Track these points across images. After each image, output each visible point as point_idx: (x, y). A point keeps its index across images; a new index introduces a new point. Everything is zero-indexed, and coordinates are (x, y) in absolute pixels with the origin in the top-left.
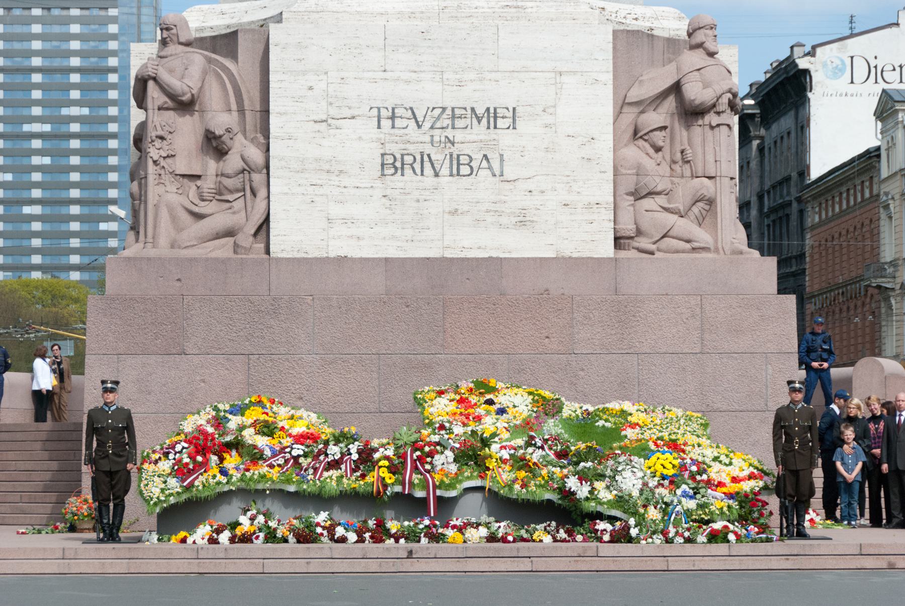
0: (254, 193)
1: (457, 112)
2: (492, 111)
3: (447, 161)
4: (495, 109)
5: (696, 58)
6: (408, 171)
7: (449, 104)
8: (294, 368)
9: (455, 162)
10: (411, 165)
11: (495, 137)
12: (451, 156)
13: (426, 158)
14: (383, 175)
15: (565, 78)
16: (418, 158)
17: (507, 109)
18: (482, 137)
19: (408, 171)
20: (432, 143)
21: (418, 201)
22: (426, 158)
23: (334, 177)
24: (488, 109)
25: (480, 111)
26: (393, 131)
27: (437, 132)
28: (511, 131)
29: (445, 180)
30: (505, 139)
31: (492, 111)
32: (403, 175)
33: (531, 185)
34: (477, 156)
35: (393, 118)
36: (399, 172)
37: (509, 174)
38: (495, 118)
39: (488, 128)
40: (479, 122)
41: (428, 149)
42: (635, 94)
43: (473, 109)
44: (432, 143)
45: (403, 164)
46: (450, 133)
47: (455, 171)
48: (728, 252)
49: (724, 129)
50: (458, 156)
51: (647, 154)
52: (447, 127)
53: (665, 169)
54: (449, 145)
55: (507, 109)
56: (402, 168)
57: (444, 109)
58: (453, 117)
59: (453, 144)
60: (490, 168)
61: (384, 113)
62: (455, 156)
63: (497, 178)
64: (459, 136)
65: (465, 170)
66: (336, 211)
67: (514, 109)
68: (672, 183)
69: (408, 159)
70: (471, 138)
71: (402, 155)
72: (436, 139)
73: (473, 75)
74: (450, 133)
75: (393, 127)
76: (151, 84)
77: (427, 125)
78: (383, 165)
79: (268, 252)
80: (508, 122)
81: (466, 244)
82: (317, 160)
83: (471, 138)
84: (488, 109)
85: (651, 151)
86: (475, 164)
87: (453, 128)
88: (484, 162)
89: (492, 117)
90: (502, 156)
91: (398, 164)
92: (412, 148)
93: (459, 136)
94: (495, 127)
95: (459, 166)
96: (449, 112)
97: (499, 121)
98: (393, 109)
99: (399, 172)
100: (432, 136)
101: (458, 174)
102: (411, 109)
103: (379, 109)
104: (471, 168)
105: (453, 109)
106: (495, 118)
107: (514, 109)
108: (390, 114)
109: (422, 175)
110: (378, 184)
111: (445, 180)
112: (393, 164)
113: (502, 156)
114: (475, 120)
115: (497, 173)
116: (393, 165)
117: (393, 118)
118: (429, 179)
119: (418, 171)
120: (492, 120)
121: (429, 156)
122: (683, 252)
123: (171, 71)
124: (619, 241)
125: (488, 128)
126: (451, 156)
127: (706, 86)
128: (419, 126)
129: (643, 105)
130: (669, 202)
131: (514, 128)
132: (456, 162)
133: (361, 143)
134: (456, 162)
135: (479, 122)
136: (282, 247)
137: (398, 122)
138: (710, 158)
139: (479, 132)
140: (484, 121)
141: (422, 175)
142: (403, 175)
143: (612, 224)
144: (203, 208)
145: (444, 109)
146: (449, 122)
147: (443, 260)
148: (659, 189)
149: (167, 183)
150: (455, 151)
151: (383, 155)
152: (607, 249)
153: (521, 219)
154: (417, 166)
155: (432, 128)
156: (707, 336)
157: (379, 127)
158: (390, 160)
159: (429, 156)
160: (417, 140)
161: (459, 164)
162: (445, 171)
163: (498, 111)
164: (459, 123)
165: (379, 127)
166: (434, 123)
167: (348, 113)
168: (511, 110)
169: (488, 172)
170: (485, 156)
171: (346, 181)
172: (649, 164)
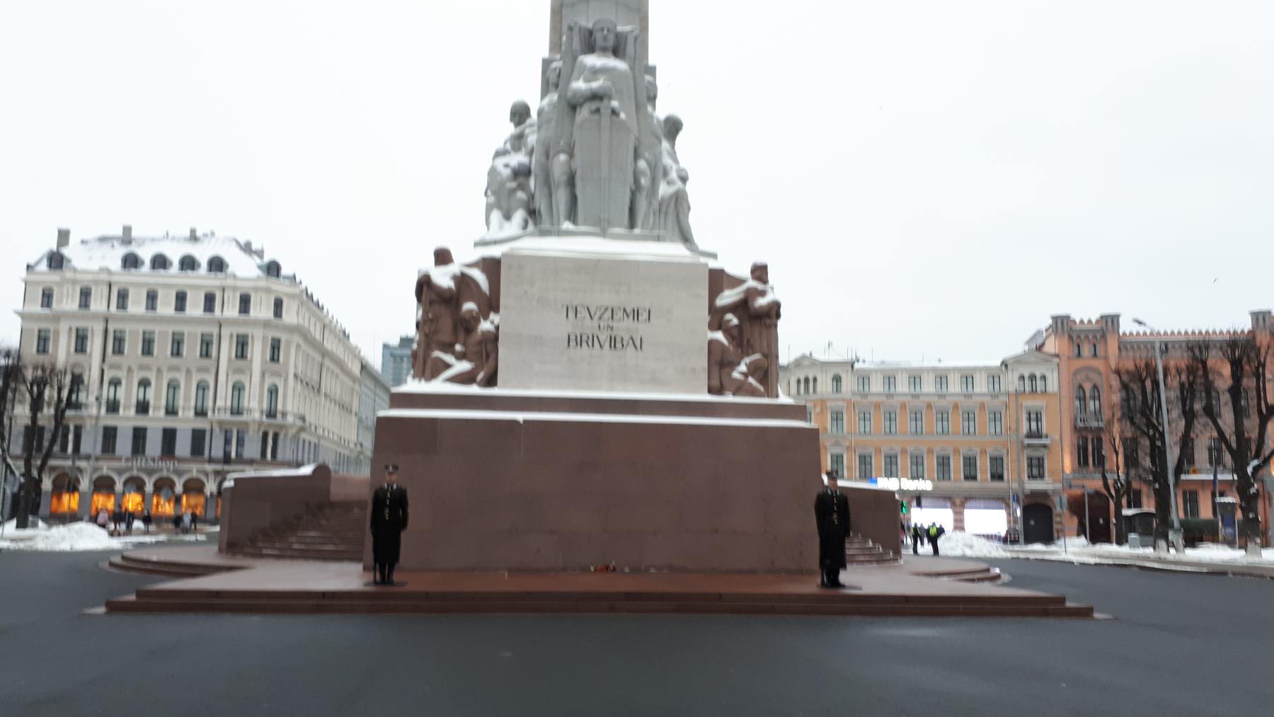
0: (488, 356)
19: (584, 344)
25: (629, 310)
41: (596, 332)
64: (615, 325)
69: (584, 338)
76: (425, 289)
77: (596, 318)
80: (646, 315)
83: (623, 326)
89: (636, 314)
116: (577, 340)
132: (613, 342)
138: (765, 344)
139: (629, 323)
160: (589, 326)
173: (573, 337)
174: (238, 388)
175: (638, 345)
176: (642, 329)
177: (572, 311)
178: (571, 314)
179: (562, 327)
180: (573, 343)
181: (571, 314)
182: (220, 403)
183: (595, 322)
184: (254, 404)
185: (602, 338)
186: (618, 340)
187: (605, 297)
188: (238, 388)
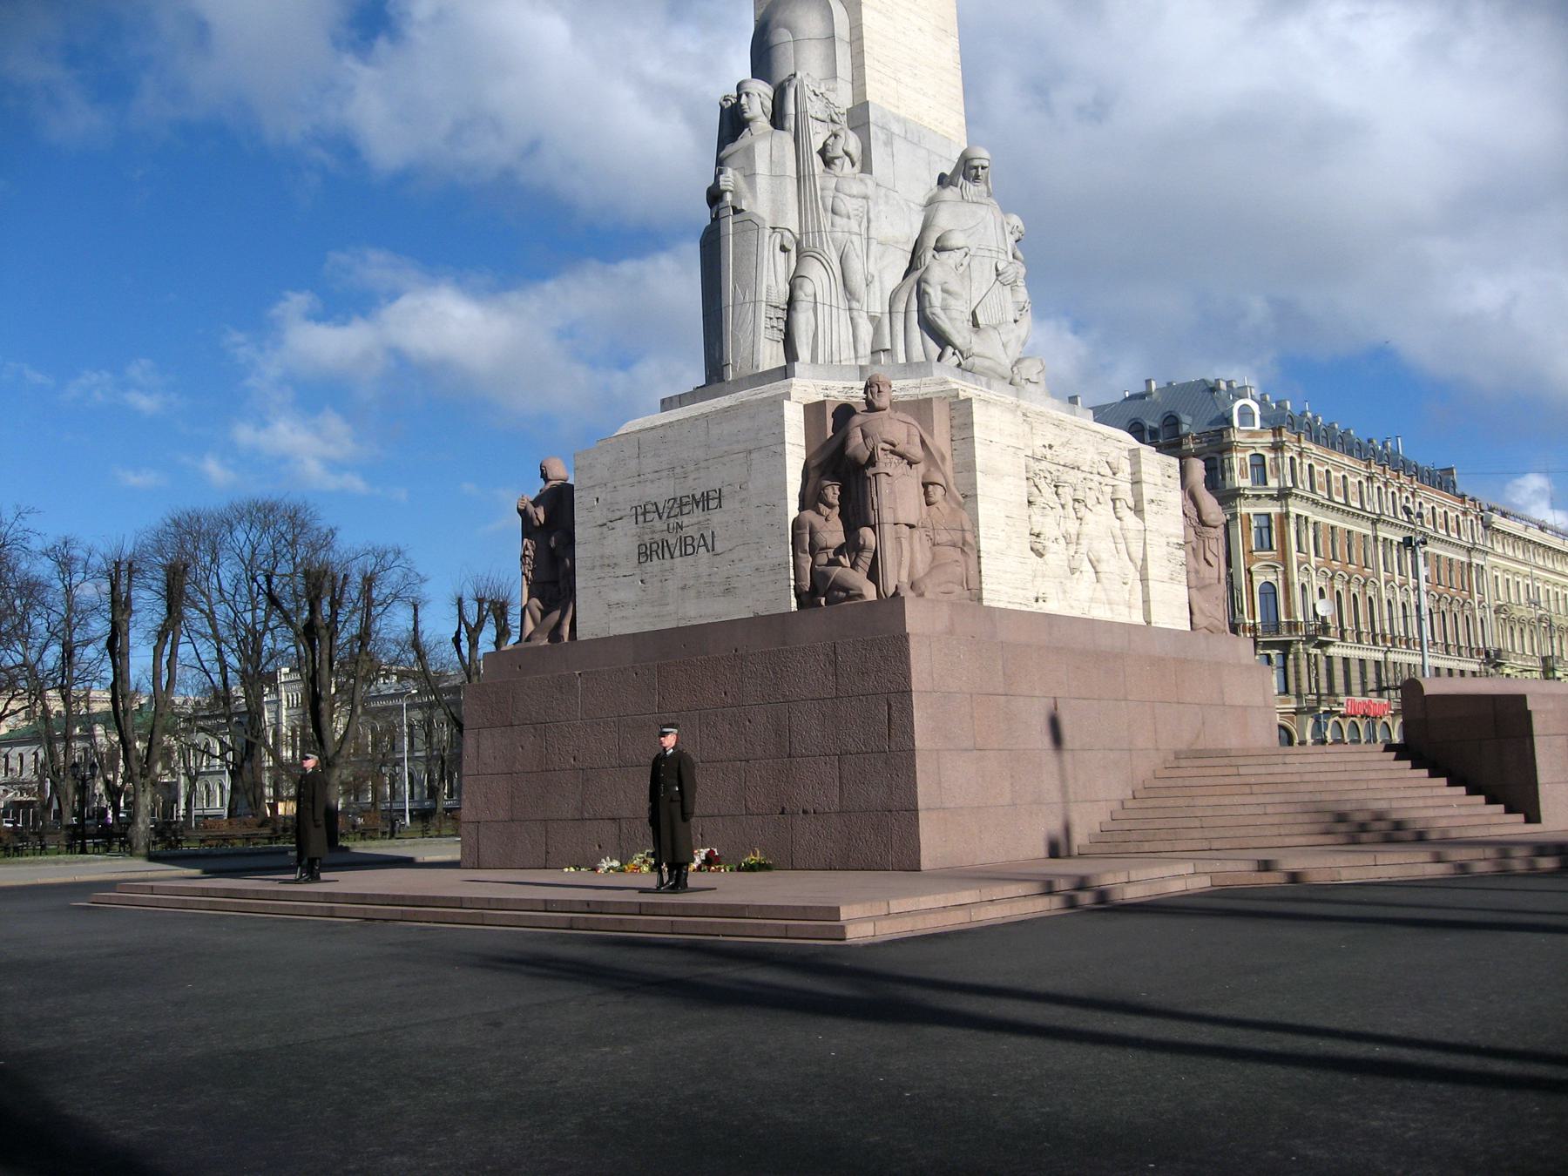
7: (678, 495)
15: (754, 455)
29: (678, 560)
30: (717, 518)
33: (734, 556)
34: (697, 536)
35: (644, 514)
37: (718, 548)
41: (666, 535)
58: (682, 505)
66: (614, 597)
70: (692, 521)
81: (692, 614)
89: (706, 498)
92: (657, 537)
93: (685, 520)
95: (687, 547)
110: (637, 571)
111: (678, 560)
116: (646, 553)
117: (644, 514)
118: (668, 563)
132: (683, 542)
133: (624, 540)
134: (683, 542)
137: (649, 517)
139: (698, 515)
147: (678, 628)
150: (683, 533)
162: (677, 553)
164: (686, 510)
167: (618, 515)
171: (620, 572)
177: (642, 512)
178: (641, 518)
181: (641, 518)
185: (672, 541)
186: (689, 541)
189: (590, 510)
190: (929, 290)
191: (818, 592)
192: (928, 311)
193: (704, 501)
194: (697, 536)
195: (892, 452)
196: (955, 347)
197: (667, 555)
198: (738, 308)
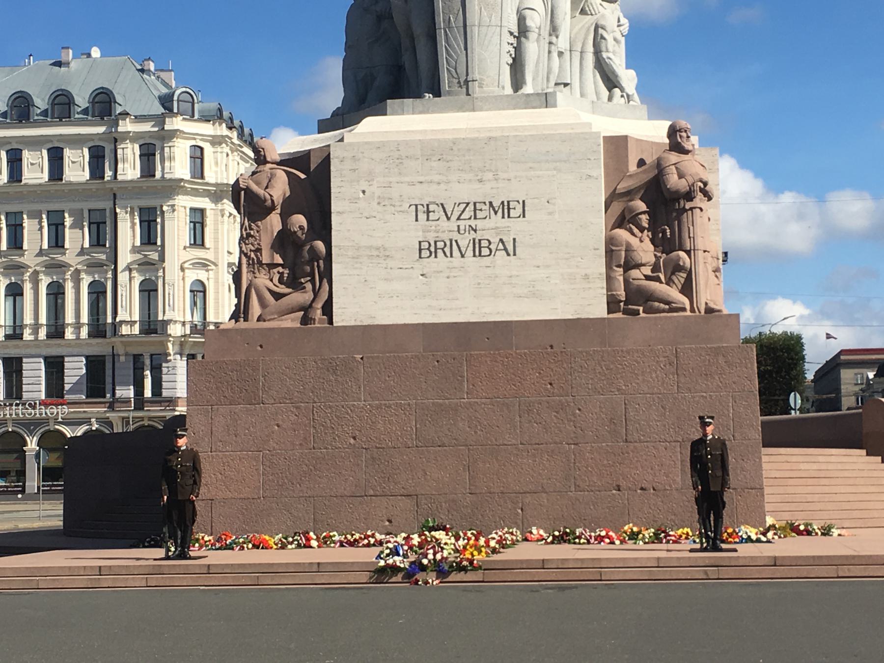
1: (478, 206)
2: (506, 204)
3: (471, 245)
4: (508, 202)
5: (674, 157)
6: (440, 252)
8: (348, 414)
9: (477, 246)
10: (443, 249)
11: (507, 224)
12: (474, 240)
13: (454, 243)
14: (420, 257)
16: (448, 243)
17: (518, 202)
18: (498, 225)
19: (440, 252)
20: (459, 231)
21: (448, 277)
22: (454, 243)
23: (381, 261)
24: (503, 203)
26: (427, 223)
27: (462, 223)
28: (521, 219)
31: (506, 204)
32: (436, 257)
34: (495, 240)
36: (433, 255)
38: (509, 209)
39: (503, 217)
40: (496, 213)
41: (455, 236)
42: (622, 187)
43: (491, 203)
44: (459, 231)
45: (436, 249)
46: (473, 223)
47: (477, 253)
48: (703, 312)
49: (698, 210)
50: (480, 241)
51: (633, 234)
52: (470, 218)
53: (648, 246)
54: (472, 232)
55: (518, 202)
56: (436, 252)
57: (468, 204)
58: (475, 210)
59: (475, 231)
60: (506, 249)
61: (420, 207)
62: (477, 241)
63: (512, 257)
64: (479, 224)
65: (485, 251)
67: (524, 202)
68: (655, 255)
69: (440, 245)
70: (490, 226)
71: (435, 242)
72: (462, 228)
73: (489, 175)
74: (473, 223)
75: (428, 219)
77: (454, 218)
78: (420, 250)
79: (331, 322)
82: (370, 248)
83: (490, 226)
84: (503, 203)
85: (636, 230)
86: (493, 247)
87: (475, 218)
88: (500, 244)
90: (514, 239)
91: (432, 249)
93: (479, 224)
94: (509, 217)
96: (471, 207)
97: (511, 211)
98: (428, 205)
99: (433, 255)
100: (459, 226)
101: (480, 255)
102: (442, 205)
103: (416, 206)
104: (491, 251)
105: (475, 204)
106: (509, 209)
107: (524, 202)
108: (425, 209)
109: (451, 256)
110: (417, 265)
112: (428, 249)
113: (514, 239)
114: (492, 212)
115: (512, 253)
116: (429, 249)
117: (428, 212)
119: (448, 254)
120: (506, 211)
121: (456, 241)
122: (664, 311)
123: (258, 183)
124: (613, 304)
125: (503, 217)
126: (474, 240)
127: (681, 176)
128: (448, 219)
129: (629, 194)
130: (653, 271)
131: (524, 216)
135: (496, 213)
136: (343, 317)
139: (497, 220)
140: (500, 210)
141: (451, 256)
142: (436, 257)
143: (605, 291)
144: (283, 289)
145: (468, 204)
146: (472, 214)
148: (643, 262)
149: (256, 271)
151: (420, 242)
152: (599, 310)
153: (531, 289)
154: (447, 250)
155: (458, 219)
156: (682, 380)
157: (417, 220)
158: (425, 245)
159: (456, 241)
160: (446, 229)
161: (480, 247)
162: (470, 253)
163: (511, 203)
165: (417, 220)
166: (461, 215)
168: (521, 202)
169: (504, 252)
170: (501, 240)
171: (391, 263)
172: (634, 241)
173: (425, 245)
174: (149, 291)
175: (510, 250)
176: (514, 227)
178: (422, 216)
179: (410, 232)
180: (425, 253)
182: (122, 316)
183: (453, 224)
184: (177, 316)
185: (463, 243)
186: (484, 243)
187: (463, 190)
188: (149, 291)
189: (354, 200)
190: (605, 35)
191: (631, 301)
192: (605, 55)
193: (506, 208)
194: (495, 240)
195: (701, 190)
196: (622, 90)
197: (456, 252)
198: (484, 30)
